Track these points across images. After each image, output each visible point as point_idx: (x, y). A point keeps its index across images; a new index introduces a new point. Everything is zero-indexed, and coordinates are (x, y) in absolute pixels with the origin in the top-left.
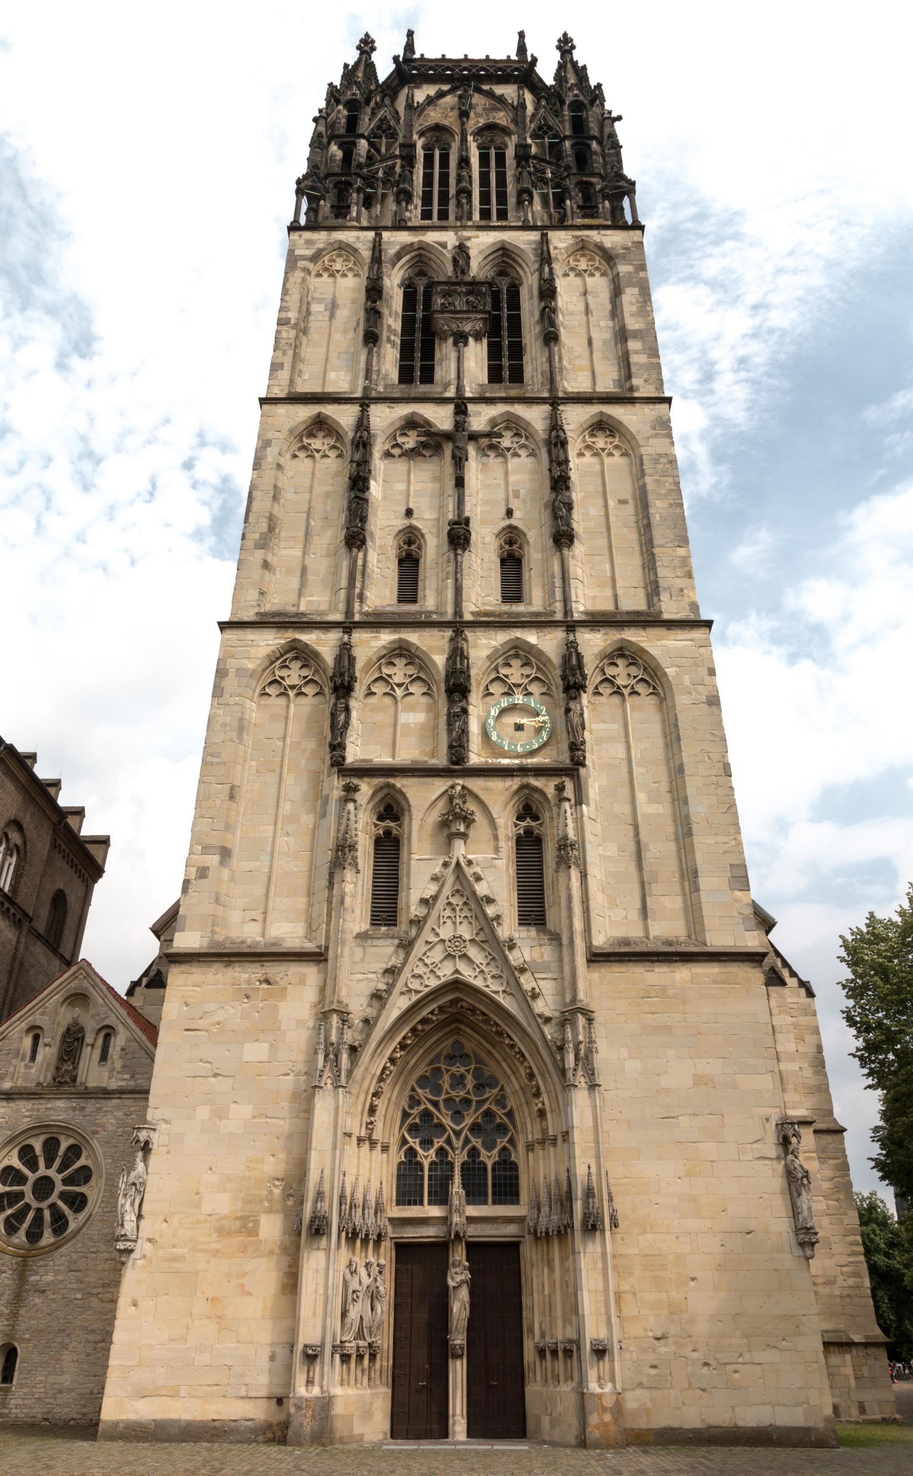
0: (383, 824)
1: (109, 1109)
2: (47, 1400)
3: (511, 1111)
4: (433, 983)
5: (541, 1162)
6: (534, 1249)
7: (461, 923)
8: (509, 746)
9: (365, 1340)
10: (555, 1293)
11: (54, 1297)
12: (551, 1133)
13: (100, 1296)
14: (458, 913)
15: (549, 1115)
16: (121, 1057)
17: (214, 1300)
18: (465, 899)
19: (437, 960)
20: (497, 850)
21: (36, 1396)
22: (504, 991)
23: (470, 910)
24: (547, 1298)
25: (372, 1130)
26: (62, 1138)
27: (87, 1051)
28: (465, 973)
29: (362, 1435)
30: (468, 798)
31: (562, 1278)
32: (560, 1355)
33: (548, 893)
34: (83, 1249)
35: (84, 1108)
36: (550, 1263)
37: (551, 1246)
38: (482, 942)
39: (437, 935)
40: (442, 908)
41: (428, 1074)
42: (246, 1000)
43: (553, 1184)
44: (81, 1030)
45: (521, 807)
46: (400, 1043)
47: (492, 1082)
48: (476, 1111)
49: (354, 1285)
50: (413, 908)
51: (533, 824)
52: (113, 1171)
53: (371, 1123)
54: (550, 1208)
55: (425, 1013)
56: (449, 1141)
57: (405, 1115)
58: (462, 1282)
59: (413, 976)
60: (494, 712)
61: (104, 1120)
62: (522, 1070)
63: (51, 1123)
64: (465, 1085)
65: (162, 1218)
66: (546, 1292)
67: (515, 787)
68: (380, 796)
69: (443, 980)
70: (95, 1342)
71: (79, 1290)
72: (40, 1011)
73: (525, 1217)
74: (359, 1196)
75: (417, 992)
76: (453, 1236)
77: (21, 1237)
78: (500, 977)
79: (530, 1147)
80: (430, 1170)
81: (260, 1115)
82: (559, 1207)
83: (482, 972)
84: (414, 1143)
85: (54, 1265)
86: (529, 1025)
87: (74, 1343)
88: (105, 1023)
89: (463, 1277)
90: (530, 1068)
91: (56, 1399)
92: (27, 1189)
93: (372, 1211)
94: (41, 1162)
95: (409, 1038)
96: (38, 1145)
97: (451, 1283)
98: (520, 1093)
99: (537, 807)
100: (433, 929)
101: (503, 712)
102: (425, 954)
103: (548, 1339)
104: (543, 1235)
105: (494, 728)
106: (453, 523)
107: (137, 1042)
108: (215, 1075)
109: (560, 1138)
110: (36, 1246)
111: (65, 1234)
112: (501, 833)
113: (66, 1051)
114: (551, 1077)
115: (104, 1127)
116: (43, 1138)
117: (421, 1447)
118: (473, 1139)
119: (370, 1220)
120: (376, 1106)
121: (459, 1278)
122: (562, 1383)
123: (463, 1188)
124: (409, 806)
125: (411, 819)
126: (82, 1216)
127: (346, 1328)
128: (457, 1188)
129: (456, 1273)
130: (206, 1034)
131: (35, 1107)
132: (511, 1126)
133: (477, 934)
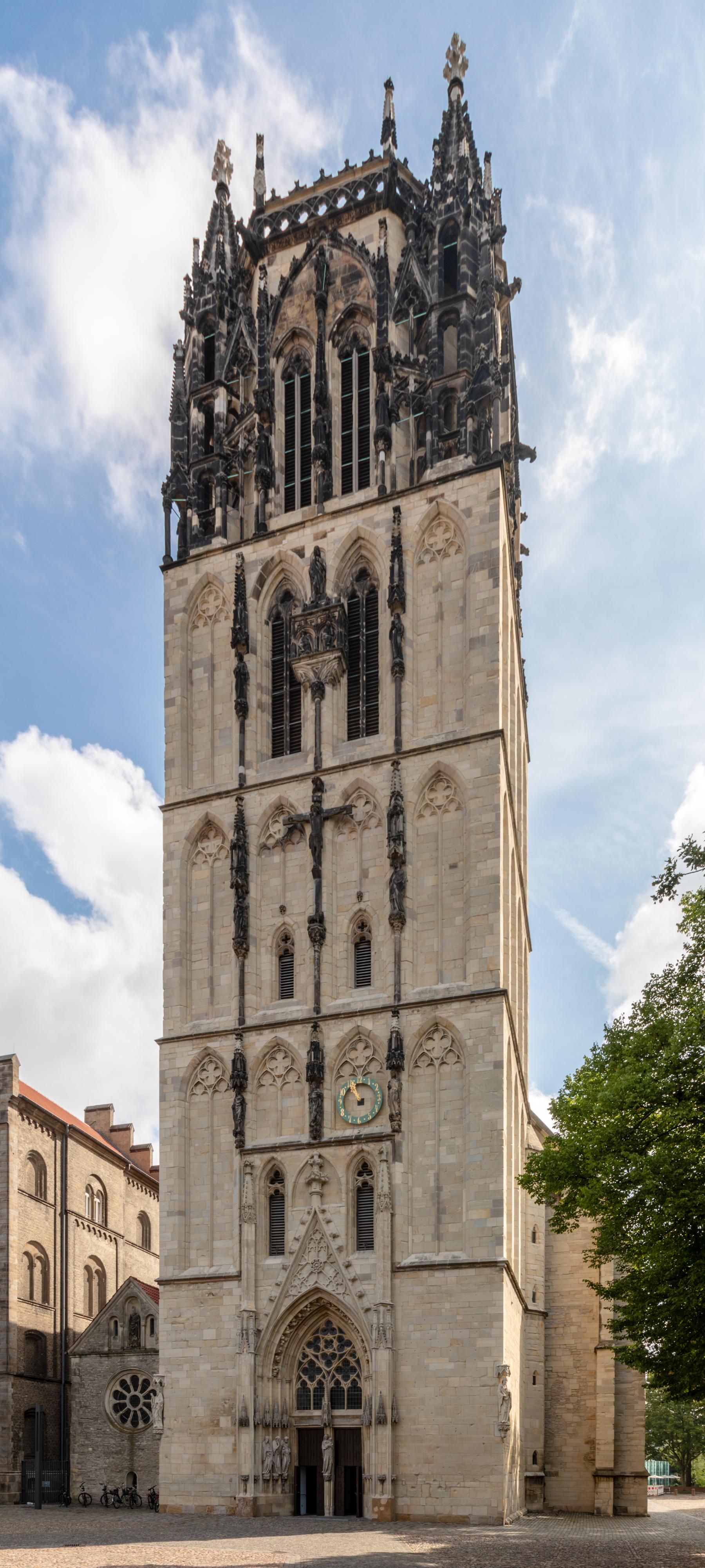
8: (353, 1118)
26: (139, 1375)
27: (143, 1328)
45: (360, 1166)
47: (349, 1343)
56: (324, 1377)
57: (300, 1363)
67: (354, 1153)
77: (128, 1424)
80: (314, 1391)
84: (305, 1378)
92: (127, 1401)
94: (132, 1388)
96: (128, 1379)
106: (311, 921)
128: (326, 1401)
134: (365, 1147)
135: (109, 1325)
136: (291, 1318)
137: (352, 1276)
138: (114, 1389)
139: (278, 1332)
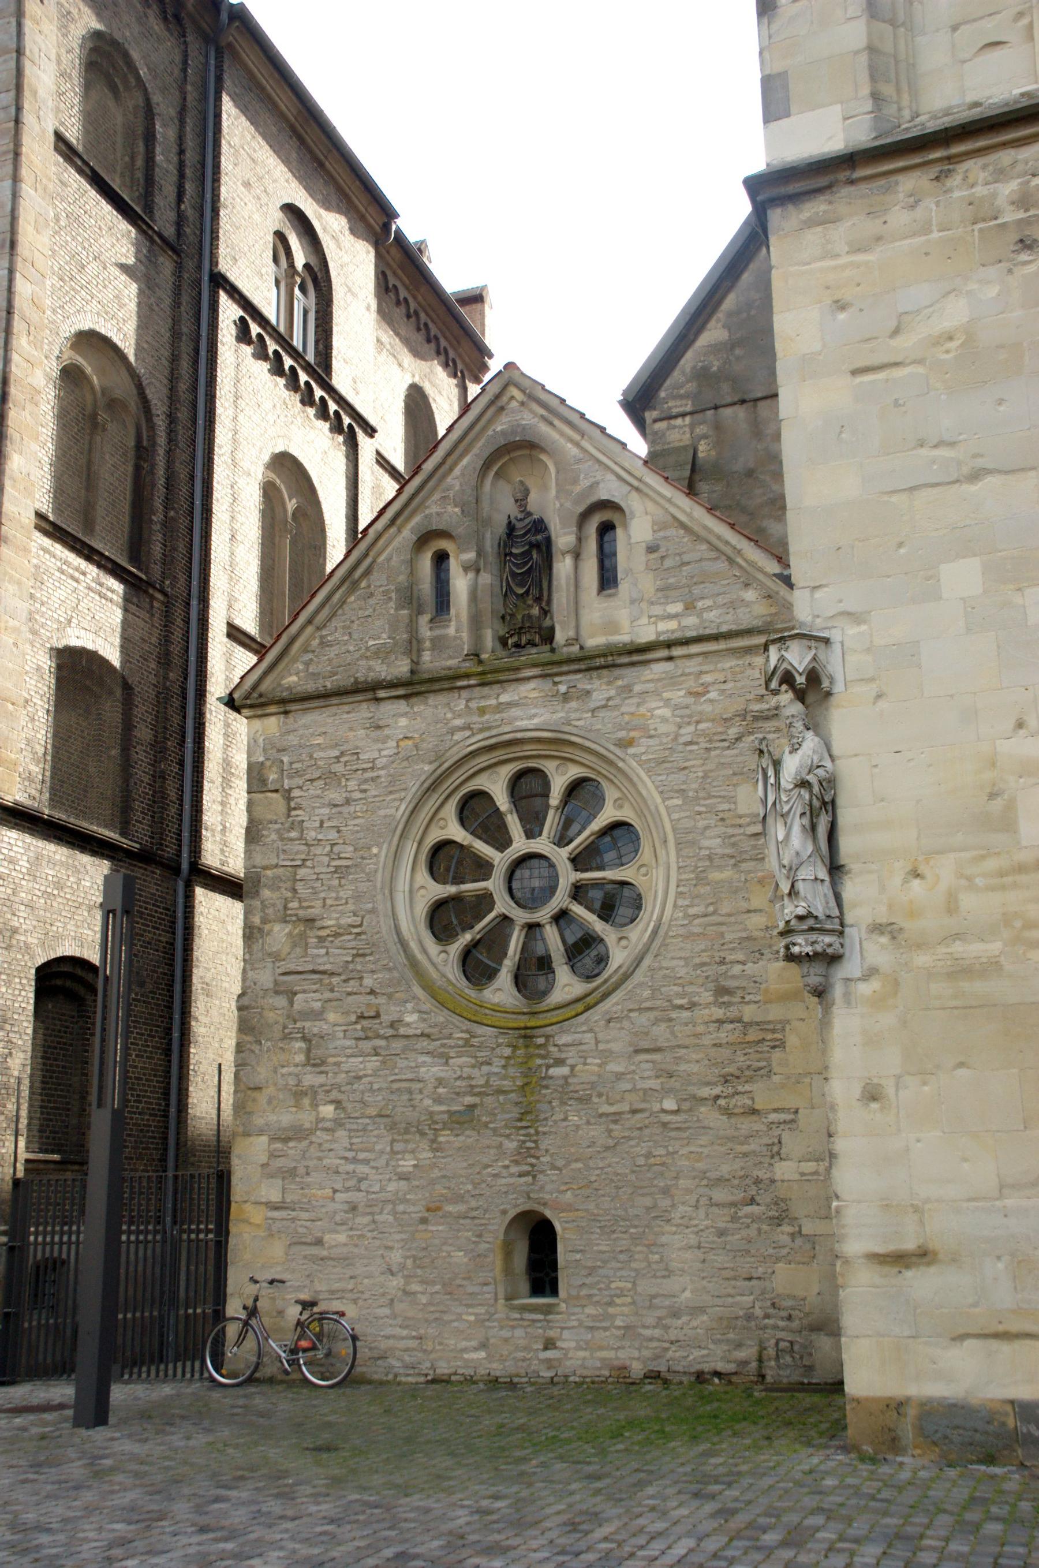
1: (650, 686)
2: (648, 1333)
11: (612, 1109)
13: (722, 1102)
16: (648, 568)
21: (618, 1323)
26: (549, 767)
27: (563, 567)
34: (658, 1003)
35: (588, 693)
44: (539, 526)
52: (688, 824)
61: (643, 710)
63: (519, 735)
65: (900, 867)
70: (733, 1204)
71: (667, 1092)
72: (436, 496)
85: (597, 1042)
87: (681, 1208)
88: (593, 499)
91: (666, 1328)
94: (514, 825)
107: (682, 525)
108: (975, 476)
110: (543, 1006)
111: (605, 975)
113: (514, 575)
115: (644, 728)
116: (506, 772)
126: (638, 933)
130: (920, 370)
131: (473, 705)
135: (412, 564)
138: (435, 836)
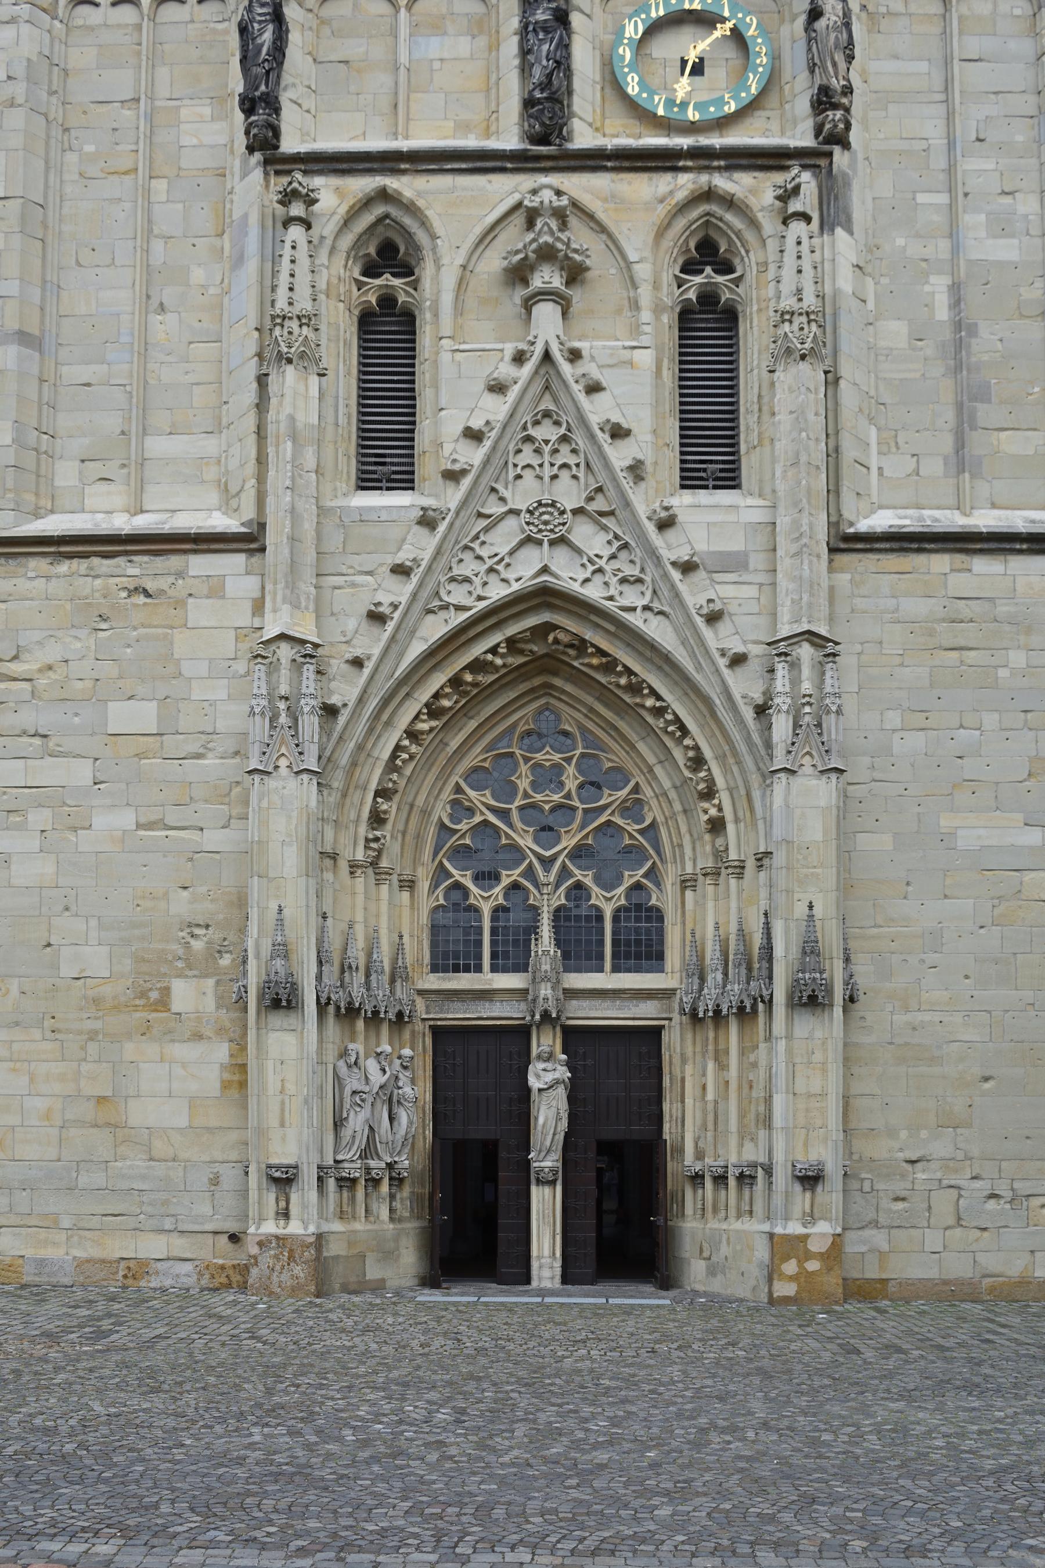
0: (378, 282)
3: (653, 825)
4: (497, 592)
5: (710, 904)
6: (689, 1036)
7: (554, 477)
9: (380, 1158)
10: (726, 1098)
12: (733, 855)
14: (547, 458)
15: (730, 828)
17: (101, 1100)
18: (563, 431)
19: (504, 550)
20: (636, 330)
22: (646, 608)
23: (574, 451)
24: (710, 1107)
25: (380, 852)
28: (564, 574)
29: (383, 1280)
30: (573, 221)
31: (740, 1078)
32: (732, 1182)
33: (747, 420)
36: (720, 1058)
37: (721, 1033)
38: (602, 514)
39: (502, 499)
40: (512, 448)
41: (486, 765)
42: (104, 626)
43: (733, 938)
45: (692, 245)
46: (427, 705)
48: (583, 827)
49: (353, 1083)
50: (448, 448)
51: (720, 279)
53: (377, 839)
54: (726, 974)
55: (477, 650)
58: (557, 1082)
59: (453, 579)
60: (633, 29)
62: (678, 754)
64: (561, 785)
66: (710, 1096)
67: (681, 195)
68: (368, 219)
69: (516, 586)
73: (675, 990)
74: (358, 954)
75: (459, 608)
76: (537, 1017)
78: (640, 581)
79: (687, 883)
81: (150, 826)
82: (744, 971)
83: (600, 570)
86: (699, 668)
89: (557, 1075)
90: (697, 748)
93: (386, 978)
95: (447, 696)
97: (534, 1083)
98: (673, 795)
99: (730, 241)
100: (493, 490)
101: (654, 29)
102: (476, 537)
103: (709, 1161)
104: (710, 1014)
105: (634, 66)
109: (751, 864)
112: (645, 294)
114: (739, 763)
117: (482, 1299)
118: (577, 872)
119: (381, 992)
120: (385, 812)
121: (549, 1077)
122: (732, 1220)
123: (558, 944)
124: (434, 237)
125: (438, 267)
127: (344, 1143)
129: (544, 1070)
132: (652, 852)
133: (590, 499)
134: (722, 182)
136: (438, 680)
137: (683, 554)
139: (388, 723)
